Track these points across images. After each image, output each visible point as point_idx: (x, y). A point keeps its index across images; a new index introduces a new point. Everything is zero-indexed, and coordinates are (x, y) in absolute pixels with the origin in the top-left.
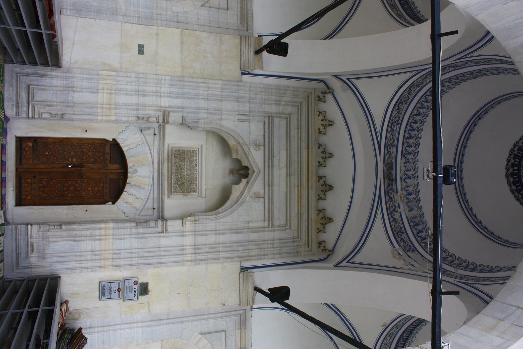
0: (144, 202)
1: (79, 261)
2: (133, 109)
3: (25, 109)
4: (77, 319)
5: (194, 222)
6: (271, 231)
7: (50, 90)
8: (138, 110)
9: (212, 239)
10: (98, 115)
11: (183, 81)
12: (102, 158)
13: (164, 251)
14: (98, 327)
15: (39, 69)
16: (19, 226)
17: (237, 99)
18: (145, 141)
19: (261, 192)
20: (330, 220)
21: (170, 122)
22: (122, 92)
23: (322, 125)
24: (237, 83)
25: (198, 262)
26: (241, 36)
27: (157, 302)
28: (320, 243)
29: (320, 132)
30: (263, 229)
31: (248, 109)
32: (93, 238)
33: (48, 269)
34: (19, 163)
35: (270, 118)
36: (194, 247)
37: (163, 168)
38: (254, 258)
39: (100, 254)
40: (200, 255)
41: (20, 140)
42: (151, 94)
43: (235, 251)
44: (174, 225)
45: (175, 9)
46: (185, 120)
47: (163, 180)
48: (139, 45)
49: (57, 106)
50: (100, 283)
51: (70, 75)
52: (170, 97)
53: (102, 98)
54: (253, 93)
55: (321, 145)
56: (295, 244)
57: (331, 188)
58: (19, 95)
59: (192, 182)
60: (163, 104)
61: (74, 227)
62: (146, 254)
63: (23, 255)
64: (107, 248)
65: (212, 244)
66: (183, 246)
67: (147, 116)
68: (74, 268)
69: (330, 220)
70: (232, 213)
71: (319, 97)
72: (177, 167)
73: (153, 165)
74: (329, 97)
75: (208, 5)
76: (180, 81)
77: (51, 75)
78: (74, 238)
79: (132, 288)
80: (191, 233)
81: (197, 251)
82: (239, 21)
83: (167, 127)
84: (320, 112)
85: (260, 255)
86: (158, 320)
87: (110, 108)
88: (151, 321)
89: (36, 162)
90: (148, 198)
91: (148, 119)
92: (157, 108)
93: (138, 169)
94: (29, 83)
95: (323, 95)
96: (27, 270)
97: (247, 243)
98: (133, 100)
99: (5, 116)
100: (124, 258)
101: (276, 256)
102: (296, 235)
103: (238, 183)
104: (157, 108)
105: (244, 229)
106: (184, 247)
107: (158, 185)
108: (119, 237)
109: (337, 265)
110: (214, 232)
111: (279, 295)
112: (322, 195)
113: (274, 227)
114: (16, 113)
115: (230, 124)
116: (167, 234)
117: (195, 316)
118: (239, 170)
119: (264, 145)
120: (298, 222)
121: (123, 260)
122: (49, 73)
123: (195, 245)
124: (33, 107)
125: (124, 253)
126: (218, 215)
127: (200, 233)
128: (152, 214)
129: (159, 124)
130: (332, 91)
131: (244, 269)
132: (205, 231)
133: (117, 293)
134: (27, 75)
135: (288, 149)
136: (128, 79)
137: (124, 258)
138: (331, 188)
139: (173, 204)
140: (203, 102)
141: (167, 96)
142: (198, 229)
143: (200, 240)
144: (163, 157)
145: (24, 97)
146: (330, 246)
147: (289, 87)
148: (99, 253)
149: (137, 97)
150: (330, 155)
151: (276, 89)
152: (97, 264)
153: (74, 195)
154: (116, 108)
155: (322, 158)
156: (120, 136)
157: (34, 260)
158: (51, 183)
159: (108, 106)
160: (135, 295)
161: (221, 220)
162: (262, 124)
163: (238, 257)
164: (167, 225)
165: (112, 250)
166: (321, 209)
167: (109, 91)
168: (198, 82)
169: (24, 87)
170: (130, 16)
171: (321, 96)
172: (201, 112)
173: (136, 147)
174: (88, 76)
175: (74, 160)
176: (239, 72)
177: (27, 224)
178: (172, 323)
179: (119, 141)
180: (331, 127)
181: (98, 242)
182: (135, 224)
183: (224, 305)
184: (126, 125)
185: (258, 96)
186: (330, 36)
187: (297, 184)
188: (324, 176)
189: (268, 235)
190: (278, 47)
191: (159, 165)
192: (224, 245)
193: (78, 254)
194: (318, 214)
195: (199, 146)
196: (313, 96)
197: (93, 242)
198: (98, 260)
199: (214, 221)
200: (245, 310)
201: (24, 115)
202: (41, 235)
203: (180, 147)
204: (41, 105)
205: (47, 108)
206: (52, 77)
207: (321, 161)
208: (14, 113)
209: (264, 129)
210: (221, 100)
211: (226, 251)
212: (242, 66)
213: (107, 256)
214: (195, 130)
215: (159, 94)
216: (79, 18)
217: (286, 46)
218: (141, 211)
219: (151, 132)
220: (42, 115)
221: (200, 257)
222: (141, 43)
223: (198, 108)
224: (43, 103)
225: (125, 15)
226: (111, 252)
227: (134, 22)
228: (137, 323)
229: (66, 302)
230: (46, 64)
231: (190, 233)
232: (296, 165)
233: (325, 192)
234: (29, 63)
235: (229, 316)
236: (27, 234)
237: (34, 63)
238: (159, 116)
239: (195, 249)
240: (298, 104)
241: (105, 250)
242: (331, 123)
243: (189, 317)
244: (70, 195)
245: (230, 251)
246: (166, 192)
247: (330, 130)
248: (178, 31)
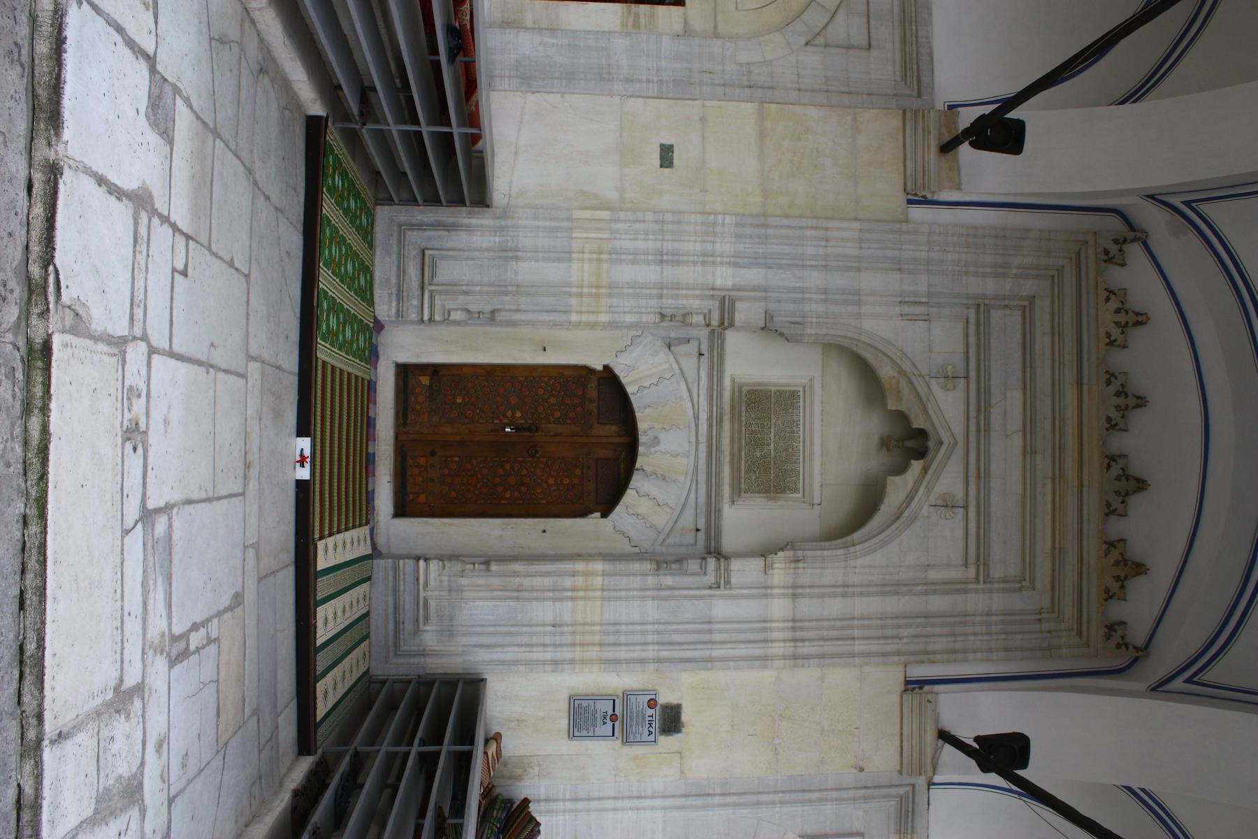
0: (676, 514)
1: (526, 645)
2: (651, 297)
3: (415, 302)
4: (519, 778)
5: (793, 565)
6: (984, 591)
7: (467, 259)
8: (661, 296)
9: (835, 607)
10: (570, 312)
11: (764, 226)
13: (721, 631)
14: (564, 800)
15: (444, 214)
16: (401, 562)
17: (898, 266)
19: (959, 494)
20: (1139, 569)
21: (737, 323)
22: (624, 257)
23: (1117, 324)
24: (897, 226)
25: (800, 661)
26: (904, 111)
27: (703, 753)
28: (1111, 628)
29: (1111, 343)
30: (963, 586)
31: (923, 288)
32: (558, 594)
33: (459, 660)
34: (401, 421)
35: (981, 308)
36: (791, 624)
38: (939, 657)
39: (574, 633)
40: (807, 644)
41: (405, 372)
42: (691, 258)
43: (892, 637)
44: (745, 571)
45: (743, 57)
46: (772, 317)
47: (719, 461)
48: (662, 145)
49: (481, 293)
50: (572, 699)
51: (509, 223)
52: (736, 265)
53: (579, 272)
54: (937, 248)
55: (1113, 375)
56: (1045, 626)
57: (1141, 485)
59: (789, 467)
60: (719, 282)
61: (517, 567)
62: (676, 638)
63: (409, 626)
64: (589, 620)
65: (834, 620)
66: (765, 621)
67: (681, 312)
68: (516, 662)
69: (1139, 569)
70: (885, 544)
71: (1106, 252)
73: (697, 426)
74: (1135, 252)
75: (820, 40)
76: (758, 226)
77: (469, 226)
78: (515, 594)
79: (644, 718)
80: (786, 591)
81: (799, 634)
82: (898, 73)
83: (730, 335)
84: (1111, 292)
85: (955, 652)
86: (699, 794)
87: (598, 295)
88: (686, 796)
89: (436, 419)
90: (685, 505)
91: (683, 318)
92: (707, 293)
93: (662, 436)
94: (424, 245)
95: (1117, 247)
96: (415, 660)
97: (923, 620)
98: (648, 274)
99: (375, 318)
100: (626, 645)
101: (995, 655)
102: (1046, 603)
103: (901, 470)
104: (707, 293)
105: (916, 585)
106: (769, 625)
107: (709, 474)
108: (618, 594)
109: (1159, 688)
110: (840, 590)
111: (1003, 755)
112: (1116, 504)
113: (991, 582)
114: (398, 311)
115: (880, 326)
117: (791, 791)
118: (903, 439)
119: (967, 377)
120: (1053, 570)
121: (623, 648)
122: (466, 221)
123: (794, 621)
124: (431, 297)
125: (627, 633)
126: (852, 549)
127: (808, 590)
128: (692, 541)
129: (709, 329)
130: (1143, 236)
131: (913, 685)
132: (819, 587)
133: (610, 724)
134: (420, 227)
135: (1028, 385)
136: (637, 226)
137: (626, 645)
138: (1141, 485)
139: (744, 519)
140: (815, 274)
141: (729, 263)
142: (802, 580)
143: (808, 607)
144: (720, 407)
145: (414, 278)
146: (1138, 635)
147: (1029, 230)
148: (570, 629)
149: (658, 268)
150: (1140, 402)
151: (996, 237)
152: (566, 654)
153: (517, 494)
154: (610, 295)
155: (1118, 408)
156: (620, 360)
157: (430, 637)
158: (468, 466)
159: (594, 291)
160: (650, 733)
161: (859, 562)
162: (960, 326)
163: (899, 653)
164: (727, 570)
165: (601, 625)
166: (1113, 539)
167: (595, 256)
168: (801, 228)
169: (414, 253)
170: (640, 81)
171: (1114, 249)
172: (810, 300)
174: (548, 224)
175: (518, 414)
176: (901, 198)
177: (418, 559)
178: (735, 805)
179: (617, 371)
180: (1140, 328)
181: (570, 604)
182: (654, 566)
183: (862, 770)
184: (633, 333)
185: (950, 256)
186: (1135, 95)
187: (1050, 475)
188: (1122, 456)
189: (976, 602)
190: (999, 132)
191: (710, 426)
192: (866, 622)
193: (525, 629)
194: (1107, 553)
195: (805, 381)
196: (1091, 252)
197: (558, 604)
198: (567, 645)
199: (842, 564)
200: (913, 786)
201: (413, 316)
202: (445, 584)
204: (447, 293)
205: (461, 298)
206: (470, 229)
207: (1114, 414)
208: (394, 311)
209: (967, 336)
210: (859, 270)
211: (868, 638)
212: (909, 183)
213: (588, 638)
214: (797, 342)
215: (711, 259)
216: (529, 95)
217: (1020, 126)
219: (692, 348)
220: (449, 314)
221: (805, 649)
222: (667, 142)
223: (802, 290)
224: (454, 288)
225: (628, 80)
226: (597, 628)
227: (650, 94)
228: (653, 797)
229: (497, 737)
230: (458, 201)
231: (782, 591)
232: (1048, 427)
233: (1124, 495)
234: (425, 201)
235: (874, 797)
236: (418, 580)
237: (433, 200)
239: (794, 629)
240: (1051, 273)
241: (584, 624)
242: (1140, 318)
243: (775, 792)
244: (508, 495)
245: (878, 638)
246: (726, 490)
247: (1139, 337)
248: (751, 108)
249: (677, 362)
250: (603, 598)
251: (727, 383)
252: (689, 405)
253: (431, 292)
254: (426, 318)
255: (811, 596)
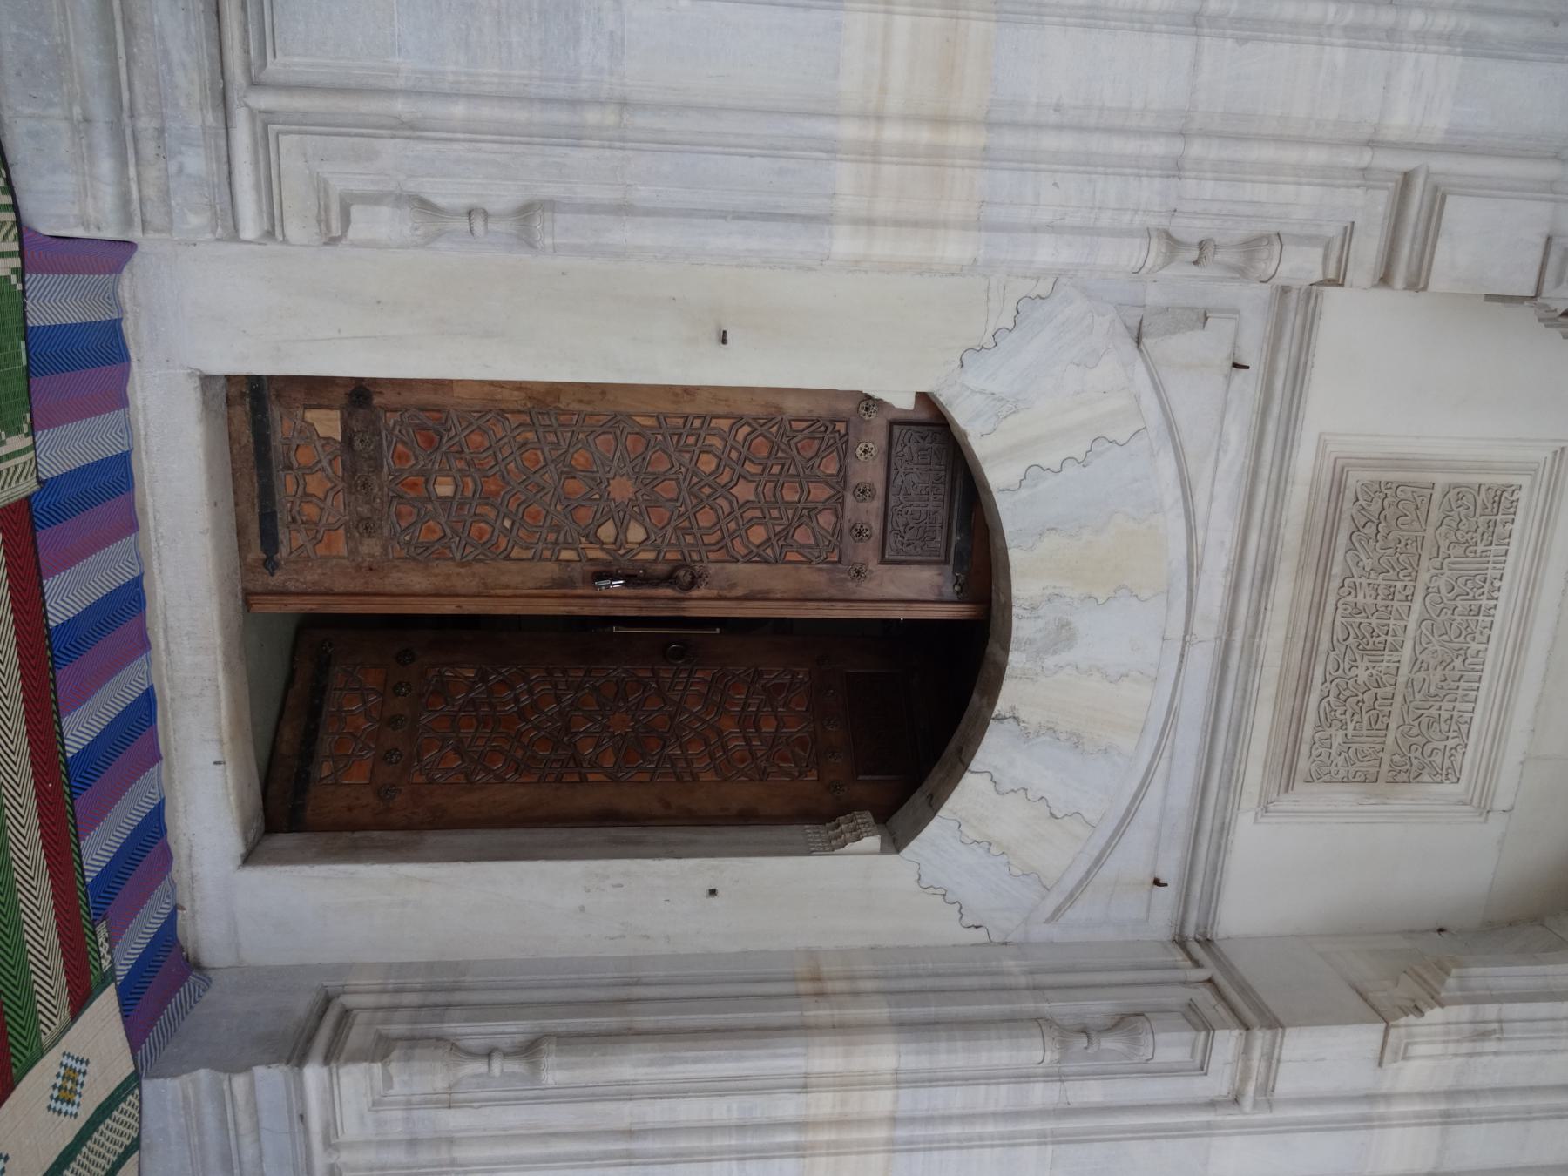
0: (1100, 840)
3: (195, 162)
5: (1466, 1047)
8: (1175, 168)
10: (819, 220)
12: (826, 520)
16: (240, 1082)
18: (1153, 416)
32: (752, 1141)
34: (256, 553)
37: (1257, 614)
49: (473, 132)
58: (128, 24)
60: (1400, 119)
61: (629, 1067)
67: (1243, 231)
72: (1358, 610)
73: (1191, 590)
87: (937, 157)
89: (370, 548)
92: (1351, 159)
104: (1351, 159)
108: (937, 1131)
114: (125, 200)
116: (1263, 1116)
124: (263, 143)
127: (1490, 1104)
141: (1446, 38)
154: (987, 158)
159: (925, 136)
164: (1271, 1060)
173: (1084, 463)
175: (636, 533)
179: (962, 415)
191: (1235, 590)
203: (1400, 463)
205: (390, 149)
208: (107, 198)
218: (1072, 897)
238: (1349, 232)
246: (1253, 774)
249: (1158, 387)
250: (892, 1147)
251: (1304, 461)
252: (1180, 527)
253: (264, 122)
254: (250, 227)
255: (1495, 1118)
